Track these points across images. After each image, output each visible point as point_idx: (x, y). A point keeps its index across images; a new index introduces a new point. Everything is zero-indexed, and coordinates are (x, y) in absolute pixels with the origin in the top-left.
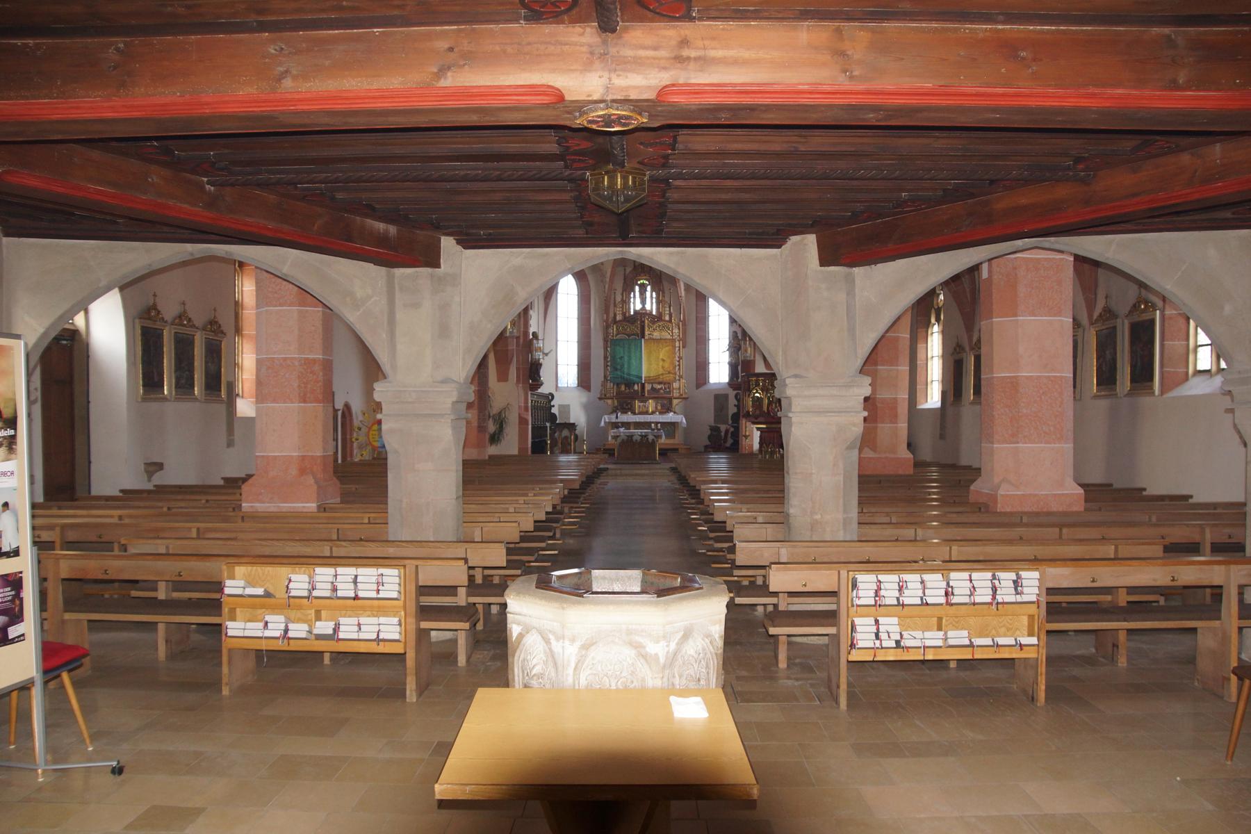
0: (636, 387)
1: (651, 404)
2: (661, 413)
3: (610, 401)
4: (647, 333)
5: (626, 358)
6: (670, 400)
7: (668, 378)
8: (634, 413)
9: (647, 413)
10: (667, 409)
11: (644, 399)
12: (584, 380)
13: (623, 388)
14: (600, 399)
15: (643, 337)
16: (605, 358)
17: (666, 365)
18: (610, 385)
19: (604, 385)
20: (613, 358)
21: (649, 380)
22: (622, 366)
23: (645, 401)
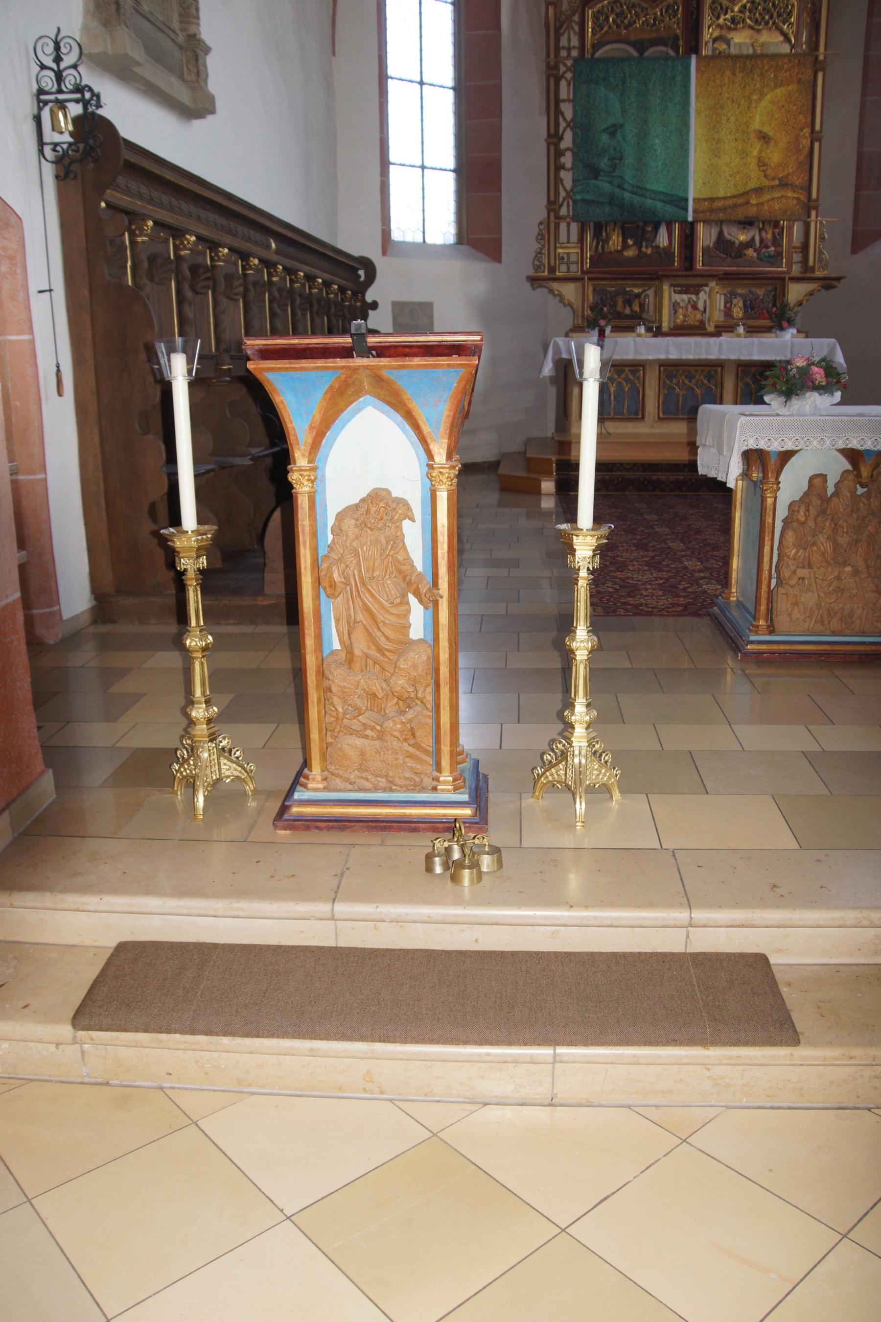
0: (662, 239)
1: (712, 299)
2: (752, 331)
3: (569, 290)
4: (708, 33)
5: (630, 130)
6: (779, 283)
7: (778, 202)
8: (658, 333)
9: (697, 330)
10: (773, 316)
11: (688, 277)
12: (479, 223)
13: (615, 241)
14: (534, 281)
15: (694, 47)
16: (554, 138)
17: (775, 156)
18: (569, 232)
19: (548, 233)
20: (583, 128)
21: (714, 211)
22: (617, 159)
23: (696, 290)
